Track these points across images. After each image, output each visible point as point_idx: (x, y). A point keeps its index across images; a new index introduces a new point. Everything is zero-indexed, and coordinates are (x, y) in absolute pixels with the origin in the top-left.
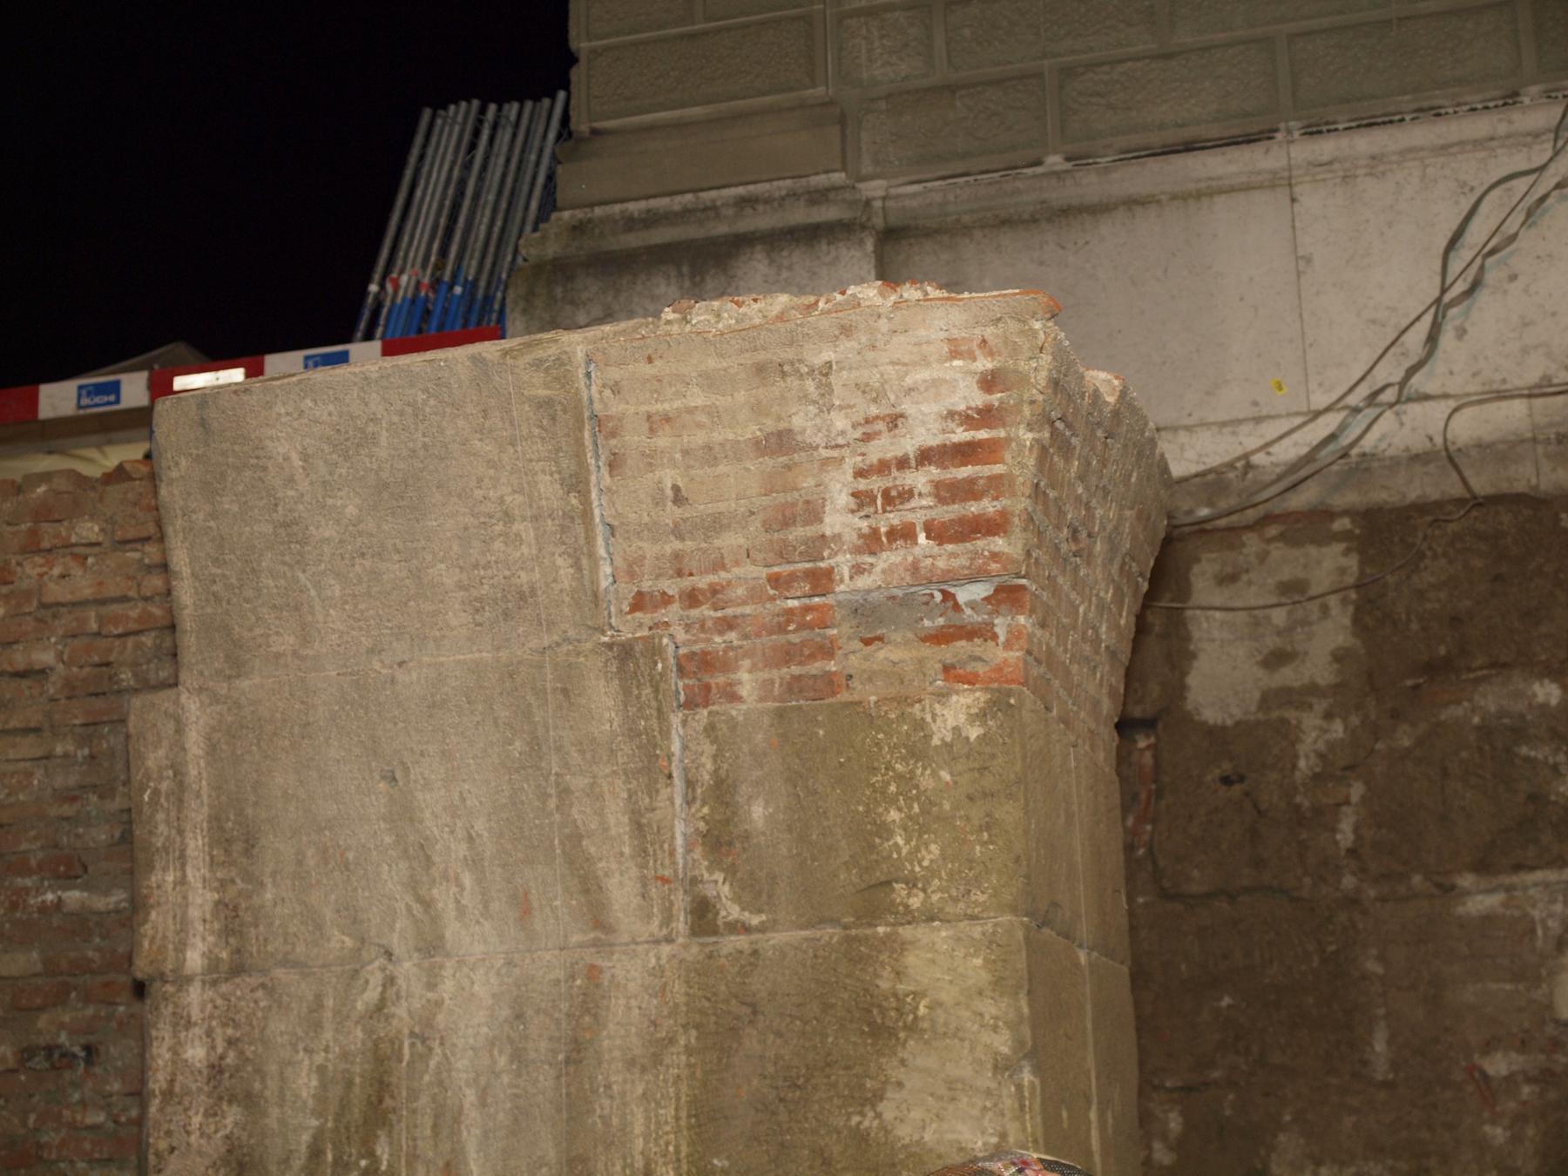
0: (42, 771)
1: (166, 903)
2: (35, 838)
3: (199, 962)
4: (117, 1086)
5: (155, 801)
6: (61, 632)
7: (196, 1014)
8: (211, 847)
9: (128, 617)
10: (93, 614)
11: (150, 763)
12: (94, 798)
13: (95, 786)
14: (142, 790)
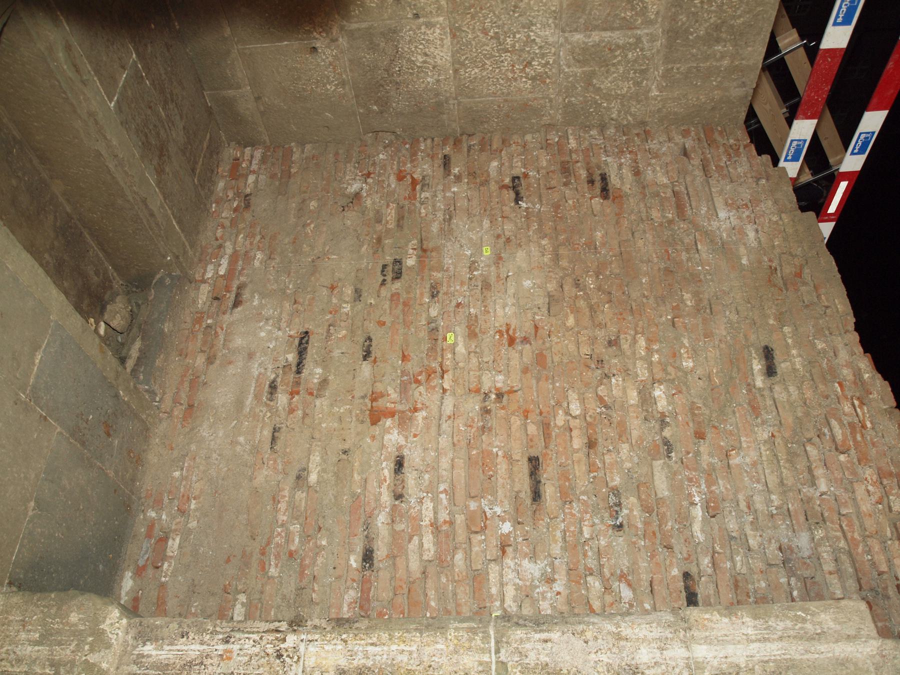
0: (761, 488)
1: (734, 629)
2: (726, 488)
3: (700, 655)
4: (603, 543)
5: (797, 619)
6: (837, 493)
7: (667, 654)
8: (775, 661)
9: (853, 532)
10: (851, 511)
11: (823, 616)
12: (750, 518)
13: (757, 519)
14: (805, 610)
